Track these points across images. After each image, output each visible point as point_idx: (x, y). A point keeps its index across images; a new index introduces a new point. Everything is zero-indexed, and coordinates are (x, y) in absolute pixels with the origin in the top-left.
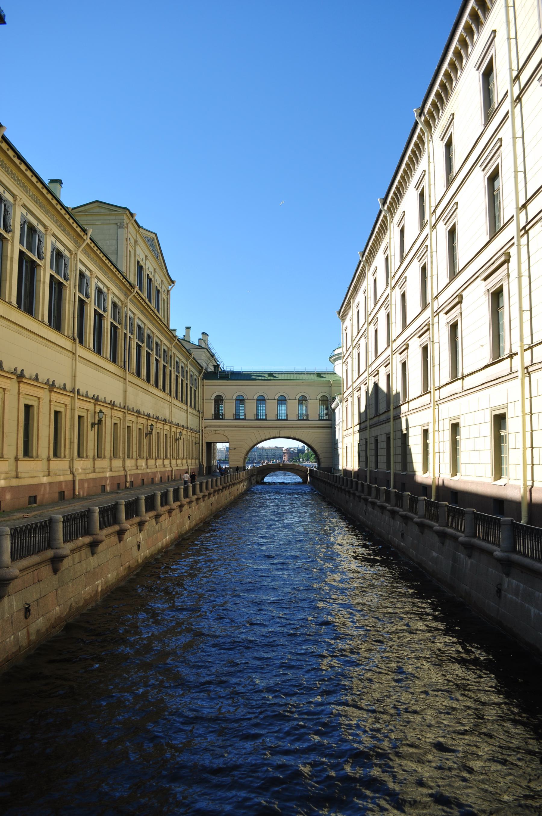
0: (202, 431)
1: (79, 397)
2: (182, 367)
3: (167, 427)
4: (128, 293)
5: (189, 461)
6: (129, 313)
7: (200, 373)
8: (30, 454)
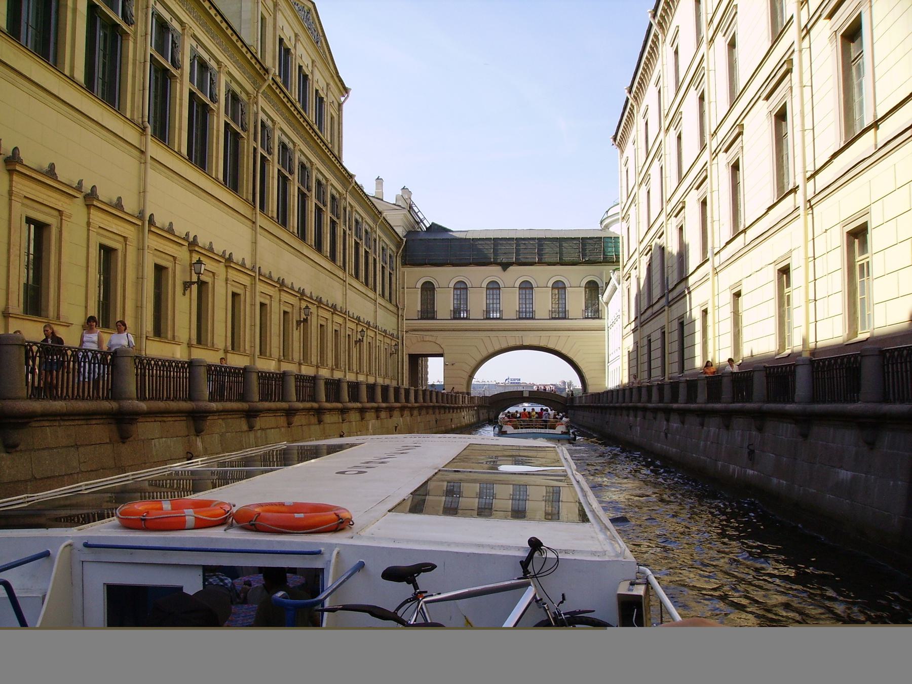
1: (153, 229)
2: (366, 232)
4: (259, 81)
6: (261, 115)
7: (398, 247)
8: (43, 313)
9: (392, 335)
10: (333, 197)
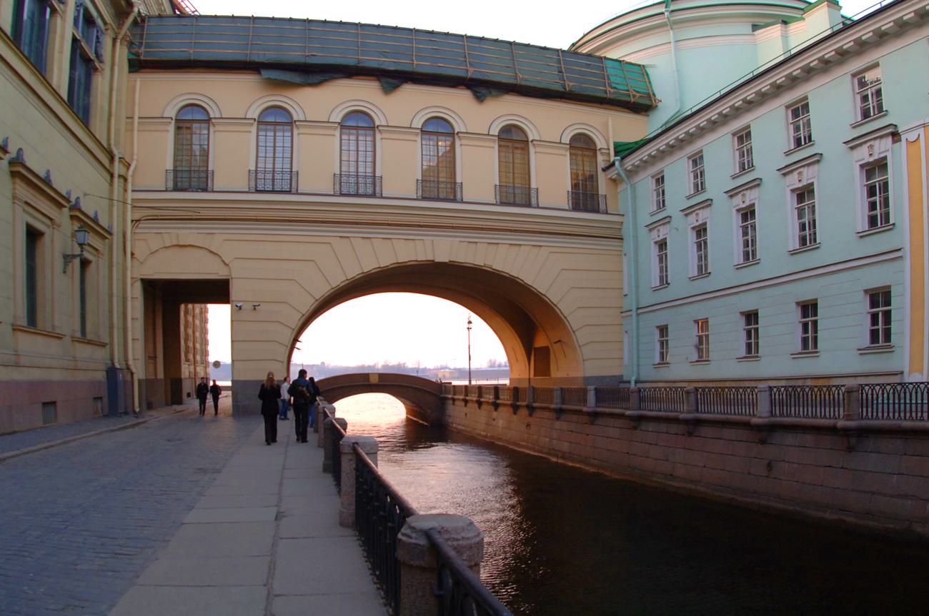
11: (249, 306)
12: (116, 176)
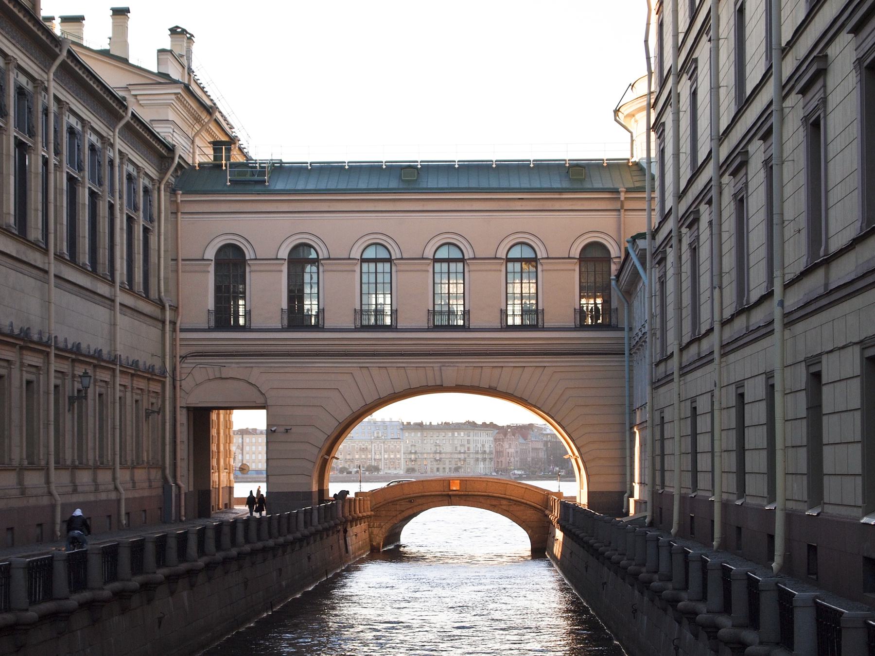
0: (174, 369)
2: (92, 147)
3: (33, 359)
5: (123, 475)
7: (163, 171)
9: (150, 370)
10: (21, 91)
11: (282, 429)
12: (168, 323)
